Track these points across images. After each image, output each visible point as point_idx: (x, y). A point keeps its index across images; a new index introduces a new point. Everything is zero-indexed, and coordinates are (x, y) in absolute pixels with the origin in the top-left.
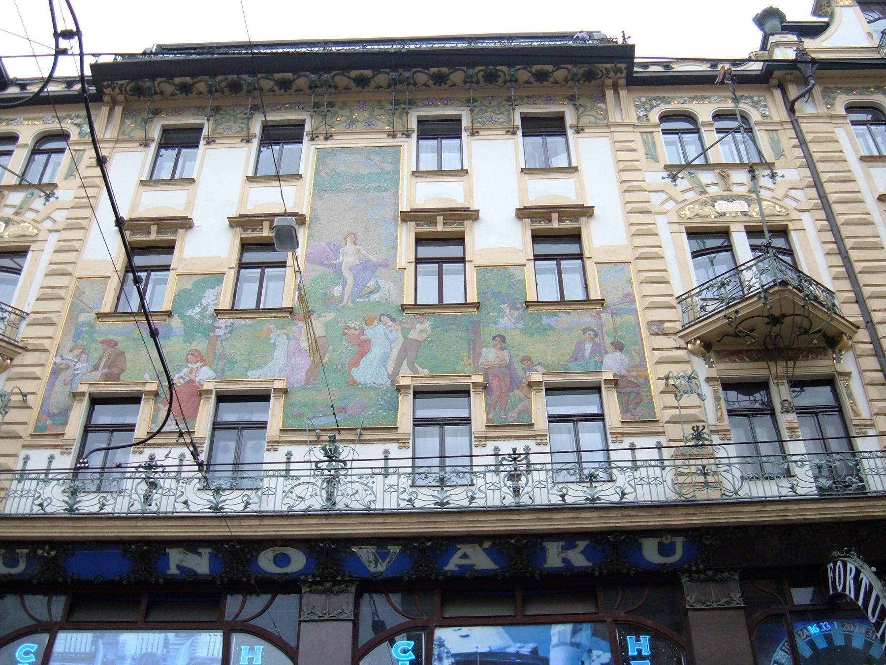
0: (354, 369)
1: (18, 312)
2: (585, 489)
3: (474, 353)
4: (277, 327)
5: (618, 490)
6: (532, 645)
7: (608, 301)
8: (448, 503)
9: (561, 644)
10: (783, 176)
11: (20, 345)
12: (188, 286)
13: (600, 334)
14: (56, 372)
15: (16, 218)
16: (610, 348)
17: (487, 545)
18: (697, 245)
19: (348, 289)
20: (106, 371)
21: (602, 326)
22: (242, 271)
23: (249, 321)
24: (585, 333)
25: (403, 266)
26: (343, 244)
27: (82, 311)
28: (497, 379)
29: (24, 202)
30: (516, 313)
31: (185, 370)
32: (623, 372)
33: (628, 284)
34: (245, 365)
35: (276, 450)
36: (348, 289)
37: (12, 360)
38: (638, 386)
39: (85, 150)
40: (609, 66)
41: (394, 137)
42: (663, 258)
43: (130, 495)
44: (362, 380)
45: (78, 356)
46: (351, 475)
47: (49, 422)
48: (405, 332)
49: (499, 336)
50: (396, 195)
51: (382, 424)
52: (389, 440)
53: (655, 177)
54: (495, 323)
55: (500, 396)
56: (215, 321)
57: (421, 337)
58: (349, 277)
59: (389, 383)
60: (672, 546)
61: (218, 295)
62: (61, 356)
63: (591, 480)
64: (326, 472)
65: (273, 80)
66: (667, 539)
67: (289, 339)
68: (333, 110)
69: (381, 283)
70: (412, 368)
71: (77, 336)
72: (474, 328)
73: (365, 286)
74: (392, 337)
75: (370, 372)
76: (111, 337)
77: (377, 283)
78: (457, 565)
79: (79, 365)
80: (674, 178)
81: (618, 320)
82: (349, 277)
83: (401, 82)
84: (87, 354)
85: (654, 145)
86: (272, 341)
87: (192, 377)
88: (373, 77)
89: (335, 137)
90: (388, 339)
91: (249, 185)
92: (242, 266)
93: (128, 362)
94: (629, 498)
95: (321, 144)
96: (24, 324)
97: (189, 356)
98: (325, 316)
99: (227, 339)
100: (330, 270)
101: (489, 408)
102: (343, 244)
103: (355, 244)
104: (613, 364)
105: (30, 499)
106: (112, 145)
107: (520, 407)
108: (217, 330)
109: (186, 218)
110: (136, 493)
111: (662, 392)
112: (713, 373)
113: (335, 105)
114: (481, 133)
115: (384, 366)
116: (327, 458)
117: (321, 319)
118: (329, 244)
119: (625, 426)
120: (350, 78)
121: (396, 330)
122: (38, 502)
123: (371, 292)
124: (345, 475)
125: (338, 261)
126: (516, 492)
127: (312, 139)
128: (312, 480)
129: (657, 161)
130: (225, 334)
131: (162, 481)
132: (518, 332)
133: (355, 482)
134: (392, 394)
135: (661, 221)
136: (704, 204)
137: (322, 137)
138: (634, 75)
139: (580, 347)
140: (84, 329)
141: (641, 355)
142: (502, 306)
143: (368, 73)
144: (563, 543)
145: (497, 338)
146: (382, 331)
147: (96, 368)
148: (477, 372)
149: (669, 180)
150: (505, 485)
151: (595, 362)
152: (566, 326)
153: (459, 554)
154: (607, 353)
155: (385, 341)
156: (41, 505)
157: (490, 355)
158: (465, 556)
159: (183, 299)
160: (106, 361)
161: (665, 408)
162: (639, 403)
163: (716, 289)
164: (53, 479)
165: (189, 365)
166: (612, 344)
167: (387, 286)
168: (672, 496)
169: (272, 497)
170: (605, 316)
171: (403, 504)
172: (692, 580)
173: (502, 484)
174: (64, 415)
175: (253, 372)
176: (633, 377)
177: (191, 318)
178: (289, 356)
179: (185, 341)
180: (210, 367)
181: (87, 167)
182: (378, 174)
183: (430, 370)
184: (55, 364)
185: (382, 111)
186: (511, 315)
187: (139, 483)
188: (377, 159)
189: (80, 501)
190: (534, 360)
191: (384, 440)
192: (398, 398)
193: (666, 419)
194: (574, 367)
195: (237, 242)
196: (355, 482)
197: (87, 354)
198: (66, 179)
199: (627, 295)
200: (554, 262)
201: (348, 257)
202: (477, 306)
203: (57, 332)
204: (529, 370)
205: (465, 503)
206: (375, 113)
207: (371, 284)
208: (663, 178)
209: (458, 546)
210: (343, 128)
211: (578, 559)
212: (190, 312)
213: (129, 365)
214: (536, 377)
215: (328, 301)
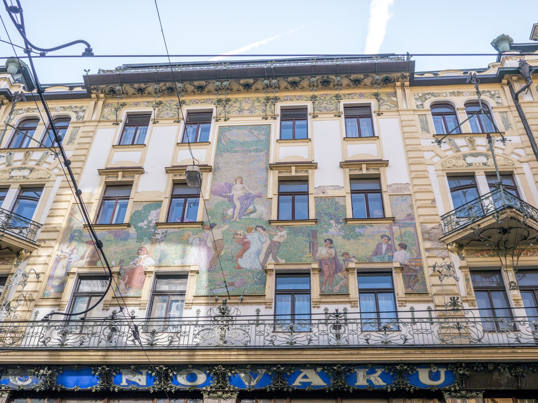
0: (239, 259)
1: (36, 224)
2: (381, 336)
4: (193, 234)
5: (402, 337)
7: (397, 217)
8: (295, 342)
10: (510, 141)
11: (36, 243)
12: (140, 209)
13: (392, 239)
15: (37, 167)
16: (398, 248)
17: (319, 369)
18: (456, 184)
19: (237, 210)
22: (173, 200)
23: (176, 230)
24: (382, 238)
25: (270, 197)
26: (234, 184)
28: (327, 266)
29: (42, 158)
30: (339, 226)
36: (237, 210)
37: (31, 252)
38: (415, 271)
39: (80, 127)
40: (399, 74)
41: (266, 119)
42: (432, 192)
43: (99, 336)
45: (72, 251)
46: (236, 324)
48: (271, 237)
49: (329, 239)
50: (268, 155)
51: (256, 293)
52: (260, 303)
53: (427, 142)
54: (327, 231)
55: (329, 276)
56: (155, 229)
57: (281, 241)
58: (238, 204)
59: (261, 268)
60: (438, 373)
61: (158, 215)
63: (385, 330)
64: (220, 323)
65: (194, 85)
68: (230, 103)
70: (275, 259)
72: (314, 234)
73: (247, 209)
74: (263, 240)
75: (249, 262)
77: (254, 207)
78: (300, 383)
80: (439, 142)
81: (403, 230)
82: (238, 204)
83: (271, 86)
84: (77, 249)
85: (427, 122)
88: (254, 83)
89: (231, 119)
90: (260, 241)
91: (178, 148)
92: (173, 196)
94: (410, 342)
95: (222, 123)
96: (40, 230)
101: (322, 284)
102: (234, 184)
103: (241, 183)
104: (400, 257)
105: (37, 338)
106: (96, 124)
107: (341, 283)
108: (157, 235)
109: (140, 168)
110: (103, 334)
111: (431, 275)
112: (464, 263)
113: (231, 100)
114: (319, 116)
116: (221, 314)
117: (221, 229)
119: (407, 296)
120: (240, 84)
121: (266, 236)
122: (41, 340)
123: (251, 213)
124: (232, 324)
125: (231, 194)
126: (338, 336)
127: (217, 121)
128: (212, 327)
129: (429, 132)
130: (161, 237)
131: (119, 327)
132: (340, 237)
133: (238, 329)
134: (262, 275)
135: (431, 169)
136: (457, 158)
137: (223, 119)
138: (415, 79)
139: (379, 247)
140: (76, 234)
141: (418, 252)
142: (331, 221)
143: (251, 81)
144: (367, 370)
145: (327, 241)
146: (257, 236)
147: (82, 258)
148: (315, 260)
149: (436, 144)
150: (331, 332)
151: (389, 256)
152: (370, 234)
153: (302, 375)
154: (396, 250)
156: (44, 342)
157: (323, 252)
158: (305, 377)
159: (137, 216)
161: (433, 285)
162: (416, 282)
163: (466, 211)
164: (52, 326)
166: (399, 245)
168: (438, 342)
169: (186, 338)
170: (395, 228)
171: (267, 343)
172: (452, 397)
173: (329, 332)
176: (412, 265)
177: (141, 228)
179: (137, 242)
181: (81, 137)
182: (257, 141)
183: (285, 260)
184: (57, 255)
185: (259, 104)
186: (336, 226)
187: (105, 329)
188: (256, 133)
189: (68, 340)
192: (266, 277)
193: (434, 292)
194: (375, 259)
195: (171, 182)
196: (238, 329)
197: (77, 249)
198: (68, 144)
199: (409, 215)
200: (364, 195)
201: (237, 192)
202: (316, 221)
205: (306, 343)
206: (255, 105)
207: (251, 208)
208: (433, 143)
209: (301, 370)
210: (236, 114)
211: (377, 380)
212: (141, 224)
214: (351, 265)
215: (224, 218)
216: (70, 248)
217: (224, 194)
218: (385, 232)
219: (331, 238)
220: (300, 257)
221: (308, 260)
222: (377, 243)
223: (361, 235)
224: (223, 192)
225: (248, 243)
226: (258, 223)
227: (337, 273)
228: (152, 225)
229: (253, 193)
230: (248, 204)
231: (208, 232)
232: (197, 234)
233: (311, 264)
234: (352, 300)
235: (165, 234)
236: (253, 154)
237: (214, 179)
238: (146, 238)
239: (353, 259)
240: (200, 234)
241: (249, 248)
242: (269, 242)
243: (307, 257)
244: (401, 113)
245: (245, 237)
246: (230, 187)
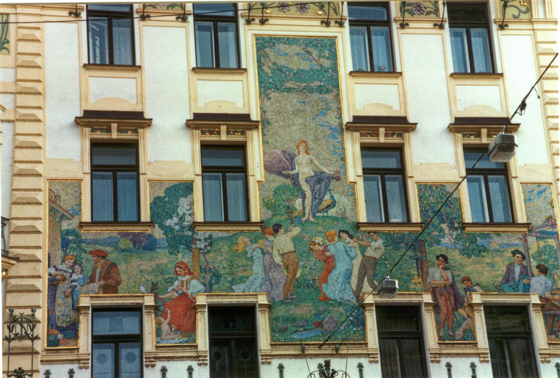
3: (422, 272)
7: (534, 224)
12: (162, 194)
13: (527, 257)
14: (53, 284)
16: (536, 271)
19: (308, 202)
20: (102, 282)
21: (528, 249)
24: (514, 255)
27: (62, 217)
31: (177, 283)
32: (548, 295)
33: (549, 207)
34: (230, 279)
35: (269, 363)
36: (308, 202)
41: (328, 24)
44: (331, 296)
45: (72, 267)
47: (60, 336)
48: (363, 249)
54: (438, 243)
55: (447, 314)
57: (377, 255)
59: (354, 301)
62: (55, 267)
67: (263, 253)
69: (336, 196)
71: (65, 245)
73: (321, 199)
76: (99, 247)
77: (332, 197)
79: (74, 277)
81: (542, 244)
82: (306, 188)
86: (249, 255)
87: (185, 290)
89: (271, 21)
90: (348, 255)
93: (122, 274)
97: (178, 269)
98: (291, 231)
99: (209, 252)
100: (288, 182)
101: (439, 325)
102: (296, 153)
108: (198, 242)
115: (349, 282)
117: (289, 234)
118: (284, 152)
119: (551, 347)
123: (329, 207)
130: (205, 247)
132: (457, 252)
137: (257, 21)
140: (70, 238)
145: (440, 258)
146: (342, 248)
148: (426, 291)
151: (524, 284)
152: (498, 247)
154: (533, 276)
155: (348, 258)
157: (437, 275)
160: (101, 272)
165: (179, 278)
166: (538, 267)
167: (343, 201)
174: (72, 330)
175: (238, 286)
178: (266, 272)
179: (171, 253)
180: (198, 280)
188: (315, 53)
190: (473, 280)
191: (357, 354)
192: (363, 314)
201: (304, 169)
203: (43, 240)
204: (470, 290)
212: (168, 222)
213: (123, 277)
216: (67, 262)
217: (284, 172)
218: (517, 245)
219: (444, 253)
220: (406, 283)
221: (417, 288)
222: (507, 263)
223: (485, 250)
224: (281, 166)
225: (332, 257)
226: (341, 226)
227: (457, 310)
228: (186, 223)
229: (327, 171)
230: (322, 191)
231: (271, 238)
232: (256, 242)
233: (421, 294)
234: (481, 351)
235: (209, 241)
236: (316, 96)
237: (265, 142)
238: (182, 246)
239: (477, 288)
240: (261, 241)
241: (334, 267)
242: (359, 258)
243: (415, 283)
244: (536, 26)
245: (326, 249)
246: (291, 158)
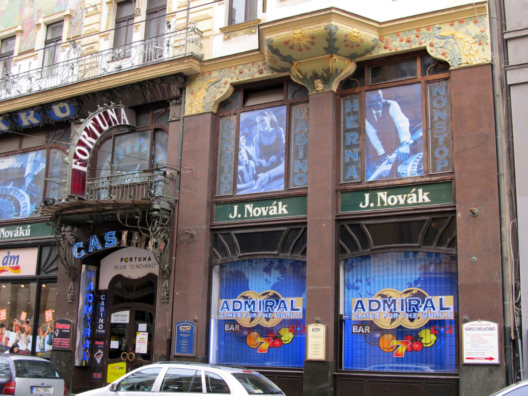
6: (22, 163)
9: (31, 161)
60: (64, 107)
66: (62, 105)
144: (25, 113)
157: (27, 12)
